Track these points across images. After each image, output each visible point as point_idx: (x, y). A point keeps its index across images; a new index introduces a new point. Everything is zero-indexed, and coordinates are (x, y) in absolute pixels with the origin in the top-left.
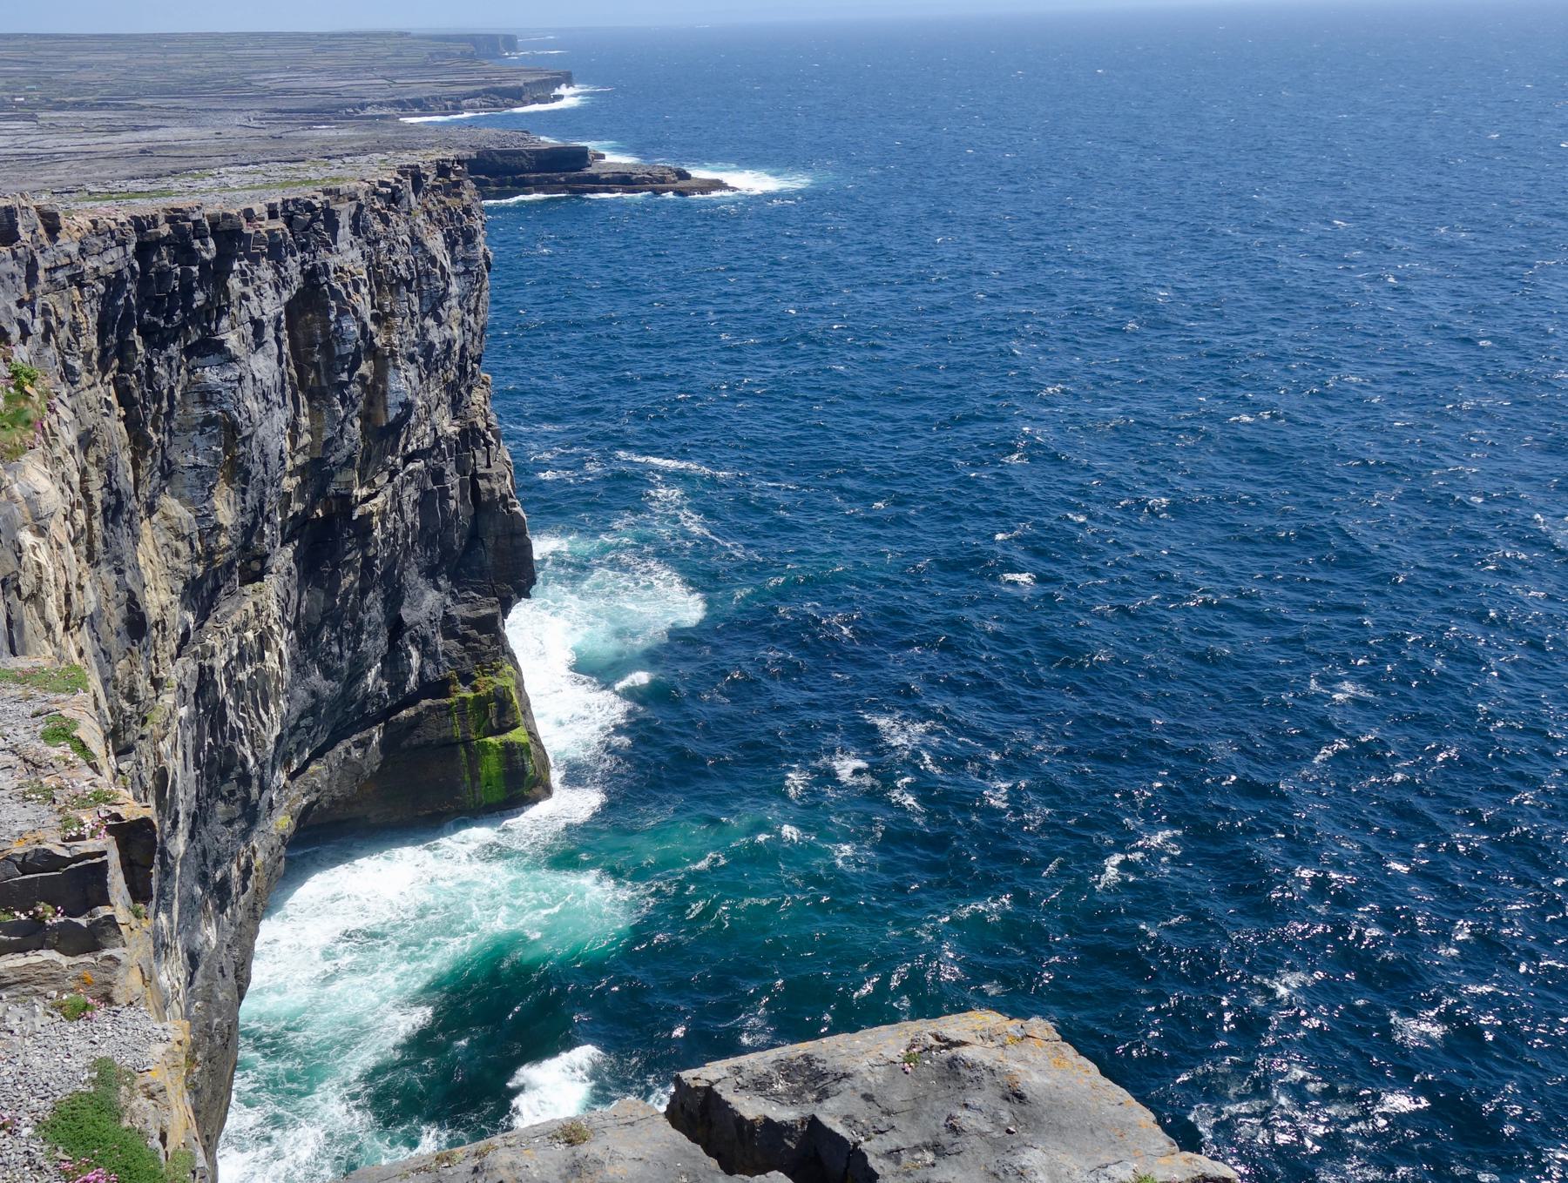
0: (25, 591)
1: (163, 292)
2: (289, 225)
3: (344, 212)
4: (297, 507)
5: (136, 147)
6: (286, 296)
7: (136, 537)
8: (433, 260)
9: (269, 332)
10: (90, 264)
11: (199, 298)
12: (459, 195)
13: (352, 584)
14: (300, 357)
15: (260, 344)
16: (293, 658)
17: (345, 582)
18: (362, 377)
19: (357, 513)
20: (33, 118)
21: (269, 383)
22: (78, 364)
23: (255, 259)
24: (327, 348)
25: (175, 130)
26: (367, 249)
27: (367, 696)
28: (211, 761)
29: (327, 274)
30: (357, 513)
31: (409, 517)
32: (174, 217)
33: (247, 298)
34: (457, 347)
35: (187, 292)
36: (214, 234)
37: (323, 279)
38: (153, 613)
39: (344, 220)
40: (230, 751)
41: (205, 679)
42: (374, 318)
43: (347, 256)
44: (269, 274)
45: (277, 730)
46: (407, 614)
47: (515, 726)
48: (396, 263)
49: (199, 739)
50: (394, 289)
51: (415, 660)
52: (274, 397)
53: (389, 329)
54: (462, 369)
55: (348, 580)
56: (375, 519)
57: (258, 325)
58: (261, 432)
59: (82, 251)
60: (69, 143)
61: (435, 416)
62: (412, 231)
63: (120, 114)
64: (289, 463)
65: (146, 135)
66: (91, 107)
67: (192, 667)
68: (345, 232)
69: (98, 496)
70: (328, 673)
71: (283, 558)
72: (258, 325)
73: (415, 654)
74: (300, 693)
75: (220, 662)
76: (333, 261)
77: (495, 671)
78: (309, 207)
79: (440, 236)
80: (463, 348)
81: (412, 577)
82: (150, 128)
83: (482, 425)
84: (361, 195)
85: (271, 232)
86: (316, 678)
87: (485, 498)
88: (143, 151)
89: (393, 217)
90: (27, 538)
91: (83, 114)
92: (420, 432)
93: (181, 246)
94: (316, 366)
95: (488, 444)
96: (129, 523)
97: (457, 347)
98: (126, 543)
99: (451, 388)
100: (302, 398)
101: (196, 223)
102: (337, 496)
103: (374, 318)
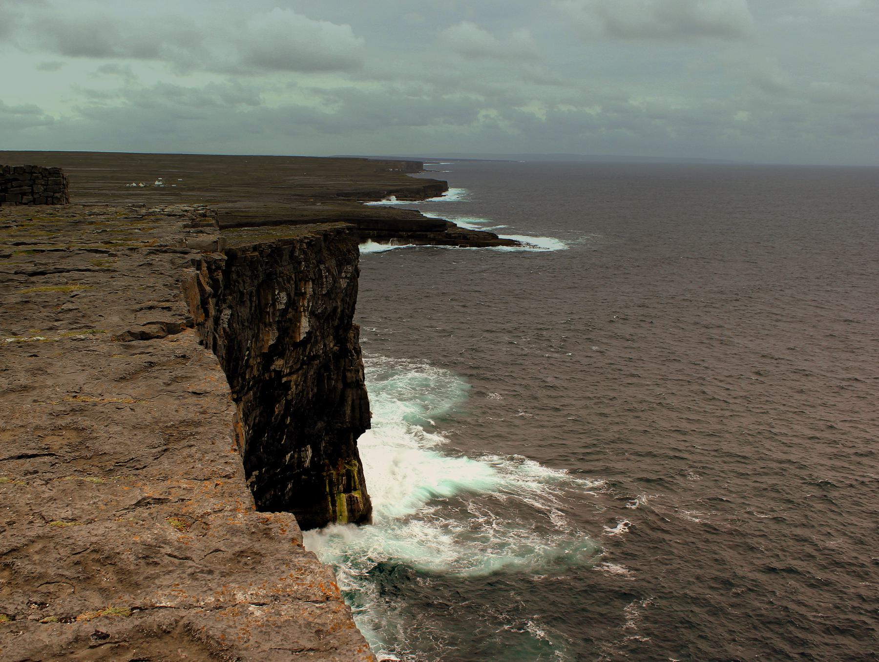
5: (224, 211)
6: (256, 283)
13: (280, 411)
19: (284, 380)
24: (274, 305)
25: (245, 203)
30: (284, 380)
33: (239, 283)
34: (339, 310)
43: (286, 268)
44: (249, 273)
50: (306, 282)
51: (310, 453)
52: (246, 324)
53: (304, 299)
54: (341, 319)
55: (278, 409)
56: (292, 383)
58: (239, 338)
65: (230, 205)
66: (207, 190)
68: (286, 257)
72: (242, 294)
74: (253, 458)
79: (334, 262)
80: (343, 311)
82: (233, 202)
83: (350, 346)
85: (252, 257)
87: (349, 381)
88: (227, 213)
91: (202, 194)
97: (339, 310)
102: (274, 370)
103: (296, 294)
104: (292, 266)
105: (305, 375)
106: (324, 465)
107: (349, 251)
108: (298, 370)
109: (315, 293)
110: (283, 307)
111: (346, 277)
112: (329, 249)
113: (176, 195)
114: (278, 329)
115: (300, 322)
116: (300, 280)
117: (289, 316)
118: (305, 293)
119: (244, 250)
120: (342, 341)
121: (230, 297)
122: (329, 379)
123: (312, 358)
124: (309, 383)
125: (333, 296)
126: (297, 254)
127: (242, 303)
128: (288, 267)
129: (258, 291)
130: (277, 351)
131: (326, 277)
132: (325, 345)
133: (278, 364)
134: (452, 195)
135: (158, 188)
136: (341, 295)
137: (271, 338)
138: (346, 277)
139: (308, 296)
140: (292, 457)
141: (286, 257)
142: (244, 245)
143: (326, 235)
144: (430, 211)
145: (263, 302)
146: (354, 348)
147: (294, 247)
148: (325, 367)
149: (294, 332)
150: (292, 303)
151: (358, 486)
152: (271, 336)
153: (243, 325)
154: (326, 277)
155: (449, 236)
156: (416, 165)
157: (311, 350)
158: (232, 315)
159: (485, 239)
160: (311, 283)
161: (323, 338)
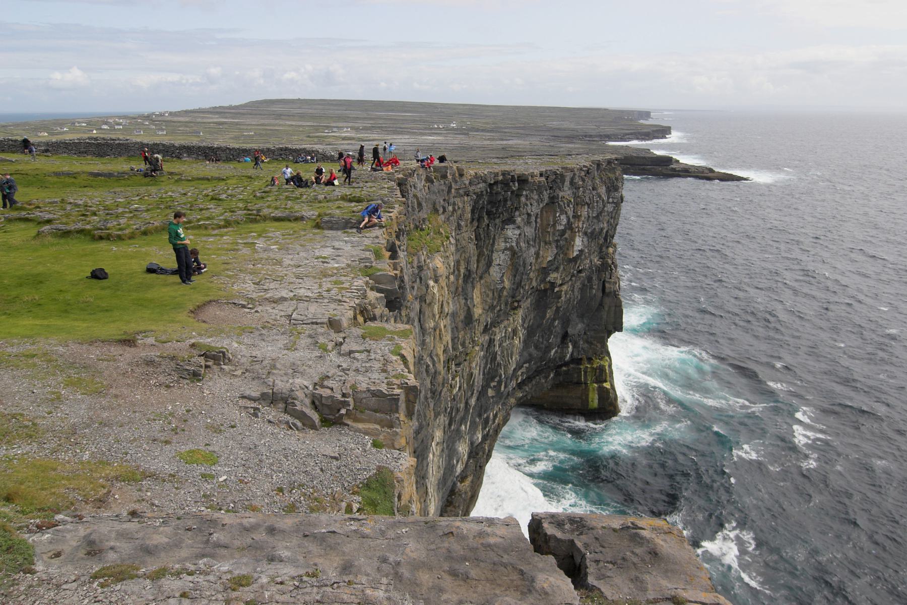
0: (428, 301)
1: (497, 200)
3: (568, 176)
4: (534, 284)
6: (541, 205)
7: (473, 288)
8: (600, 196)
9: (533, 218)
10: (471, 189)
12: (615, 173)
16: (525, 341)
17: (548, 316)
18: (566, 239)
19: (556, 289)
20: (467, 134)
22: (463, 223)
24: (554, 225)
27: (550, 359)
28: (489, 373)
30: (556, 289)
31: (576, 293)
32: (504, 174)
35: (506, 200)
36: (518, 181)
37: (556, 200)
38: (476, 316)
39: (568, 179)
40: (497, 370)
41: (491, 342)
43: (566, 193)
44: (536, 197)
45: (514, 366)
46: (570, 331)
47: (606, 381)
49: (486, 364)
51: (570, 349)
54: (606, 239)
55: (549, 314)
59: (470, 183)
60: (478, 143)
63: (498, 134)
65: (505, 142)
66: (488, 131)
67: (487, 338)
68: (567, 183)
69: (462, 271)
70: (536, 347)
71: (526, 304)
72: (529, 215)
73: (571, 347)
74: (525, 354)
75: (498, 337)
76: (561, 194)
77: (601, 359)
79: (604, 188)
80: (607, 232)
81: (574, 317)
83: (610, 262)
85: (540, 182)
86: (532, 349)
87: (607, 290)
90: (431, 283)
93: (506, 184)
95: (611, 270)
96: (472, 283)
98: (470, 289)
100: (542, 244)
101: (513, 176)
102: (549, 282)
103: (574, 217)
105: (573, 286)
106: (581, 359)
107: (617, 179)
108: (568, 282)
110: (562, 227)
111: (613, 202)
113: (465, 134)
114: (557, 247)
115: (574, 241)
117: (566, 236)
120: (603, 256)
121: (519, 219)
122: (591, 288)
123: (580, 272)
124: (576, 293)
126: (576, 181)
127: (528, 223)
129: (541, 212)
130: (552, 266)
131: (597, 202)
132: (591, 261)
133: (553, 276)
134: (674, 137)
135: (453, 129)
136: (607, 218)
137: (549, 255)
138: (613, 202)
139: (583, 218)
140: (556, 352)
141: (567, 183)
142: (531, 171)
143: (599, 165)
144: (658, 149)
147: (574, 175)
148: (590, 279)
150: (569, 226)
151: (608, 379)
152: (550, 253)
154: (597, 202)
155: (674, 170)
156: (646, 114)
158: (520, 235)
159: (703, 172)
161: (590, 254)
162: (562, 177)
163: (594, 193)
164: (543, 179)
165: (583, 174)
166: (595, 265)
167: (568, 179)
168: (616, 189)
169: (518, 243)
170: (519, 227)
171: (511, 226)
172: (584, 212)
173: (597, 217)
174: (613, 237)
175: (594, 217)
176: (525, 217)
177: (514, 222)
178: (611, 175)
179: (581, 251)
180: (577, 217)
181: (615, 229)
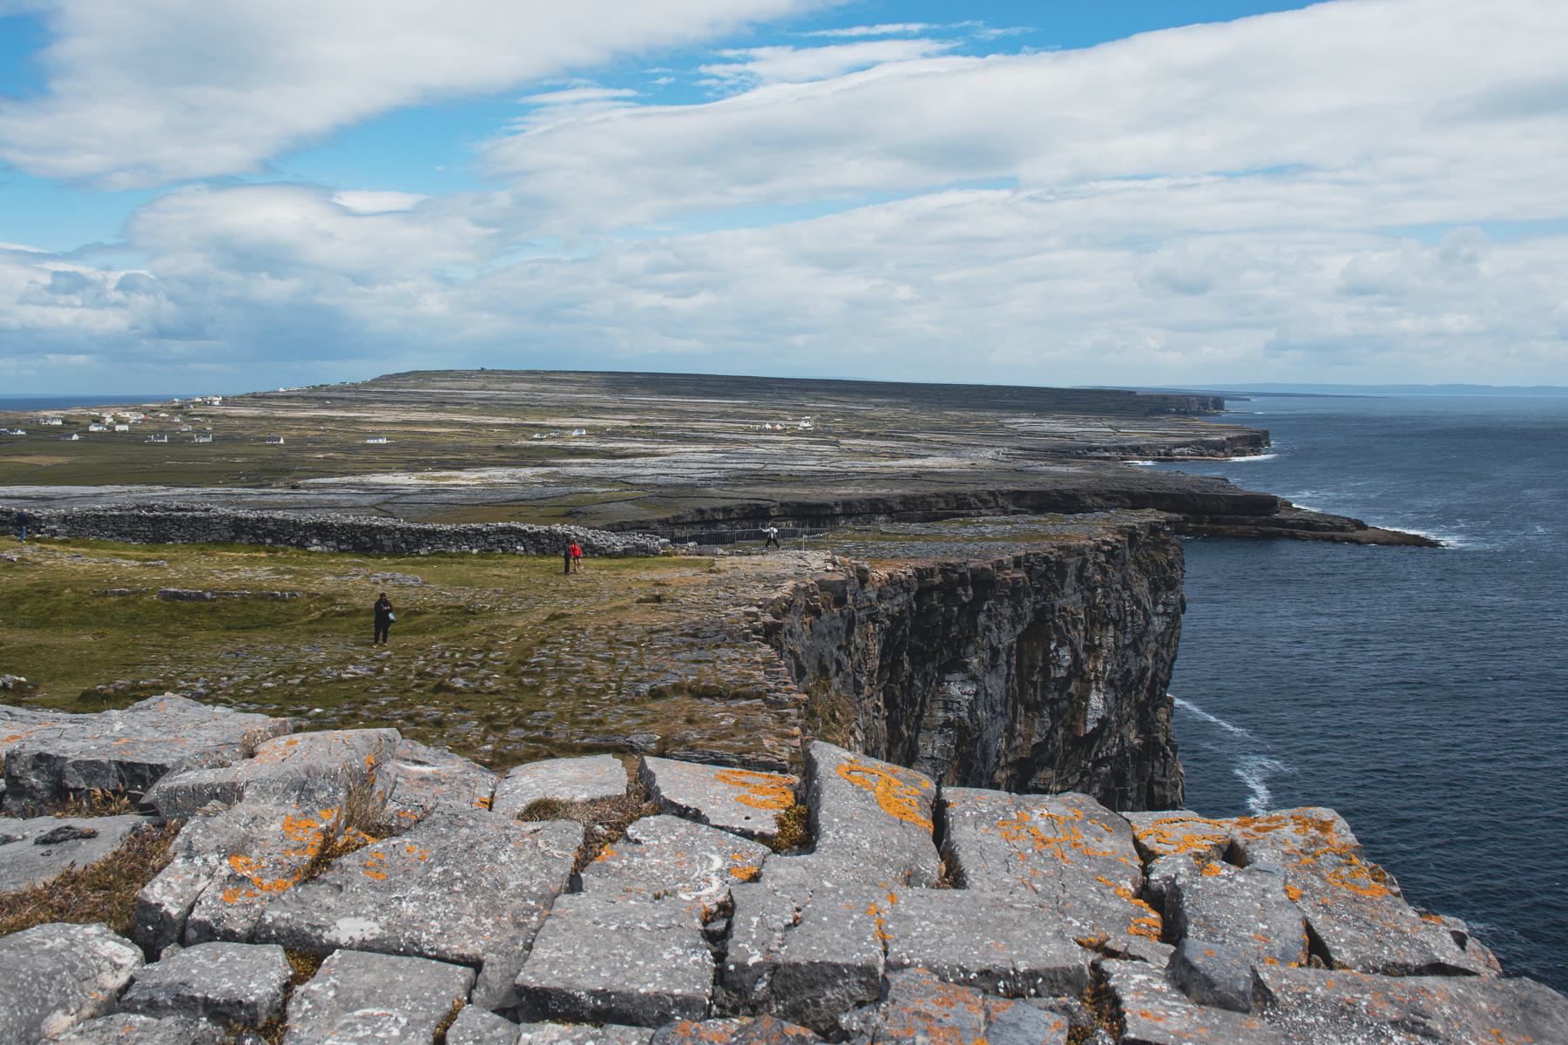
2: (1028, 572)
3: (1073, 562)
6: (1020, 629)
8: (1138, 603)
11: (955, 630)
12: (1166, 552)
14: (1023, 677)
15: (994, 666)
18: (1070, 695)
21: (997, 697)
23: (1000, 600)
24: (1045, 671)
26: (1086, 593)
29: (1053, 612)
33: (990, 630)
34: (1149, 674)
35: (948, 624)
37: (1049, 616)
39: (1072, 570)
42: (1086, 648)
43: (1070, 600)
44: (1008, 612)
48: (1108, 606)
50: (1104, 626)
52: (999, 709)
53: (1097, 658)
54: (1151, 690)
57: (995, 652)
58: (985, 737)
61: (1124, 731)
62: (1124, 578)
64: (1002, 761)
68: (1071, 579)
72: (995, 652)
78: (1046, 560)
79: (1146, 584)
80: (1155, 675)
83: (1162, 739)
84: (1087, 550)
89: (1111, 570)
92: (1110, 742)
94: (1034, 684)
95: (1166, 756)
97: (1149, 674)
99: (1141, 708)
100: (1021, 709)
103: (1086, 648)
104: (1079, 596)
107: (1171, 564)
109: (1117, 647)
111: (1165, 613)
112: (1139, 563)
115: (1087, 699)
116: (1092, 622)
117: (1072, 689)
118: (1100, 645)
119: (1000, 566)
121: (975, 661)
123: (1098, 763)
125: (1142, 648)
128: (1074, 598)
132: (1122, 739)
138: (1165, 613)
141: (1071, 579)
142: (997, 557)
145: (1026, 662)
146: (1168, 740)
149: (1073, 717)
150: (1076, 671)
153: (994, 711)
157: (1100, 750)
158: (976, 694)
160: (1111, 628)
162: (1061, 567)
163: (1126, 595)
164: (1020, 574)
165: (1102, 558)
166: (1132, 749)
167: (1072, 570)
168: (1171, 585)
169: (972, 711)
170: (974, 679)
171: (959, 676)
172: (1108, 638)
173: (1134, 646)
174: (1166, 685)
175: (1126, 647)
176: (986, 655)
177: (964, 668)
178: (1160, 558)
179: (1103, 722)
180: (1092, 649)
181: (1171, 668)
